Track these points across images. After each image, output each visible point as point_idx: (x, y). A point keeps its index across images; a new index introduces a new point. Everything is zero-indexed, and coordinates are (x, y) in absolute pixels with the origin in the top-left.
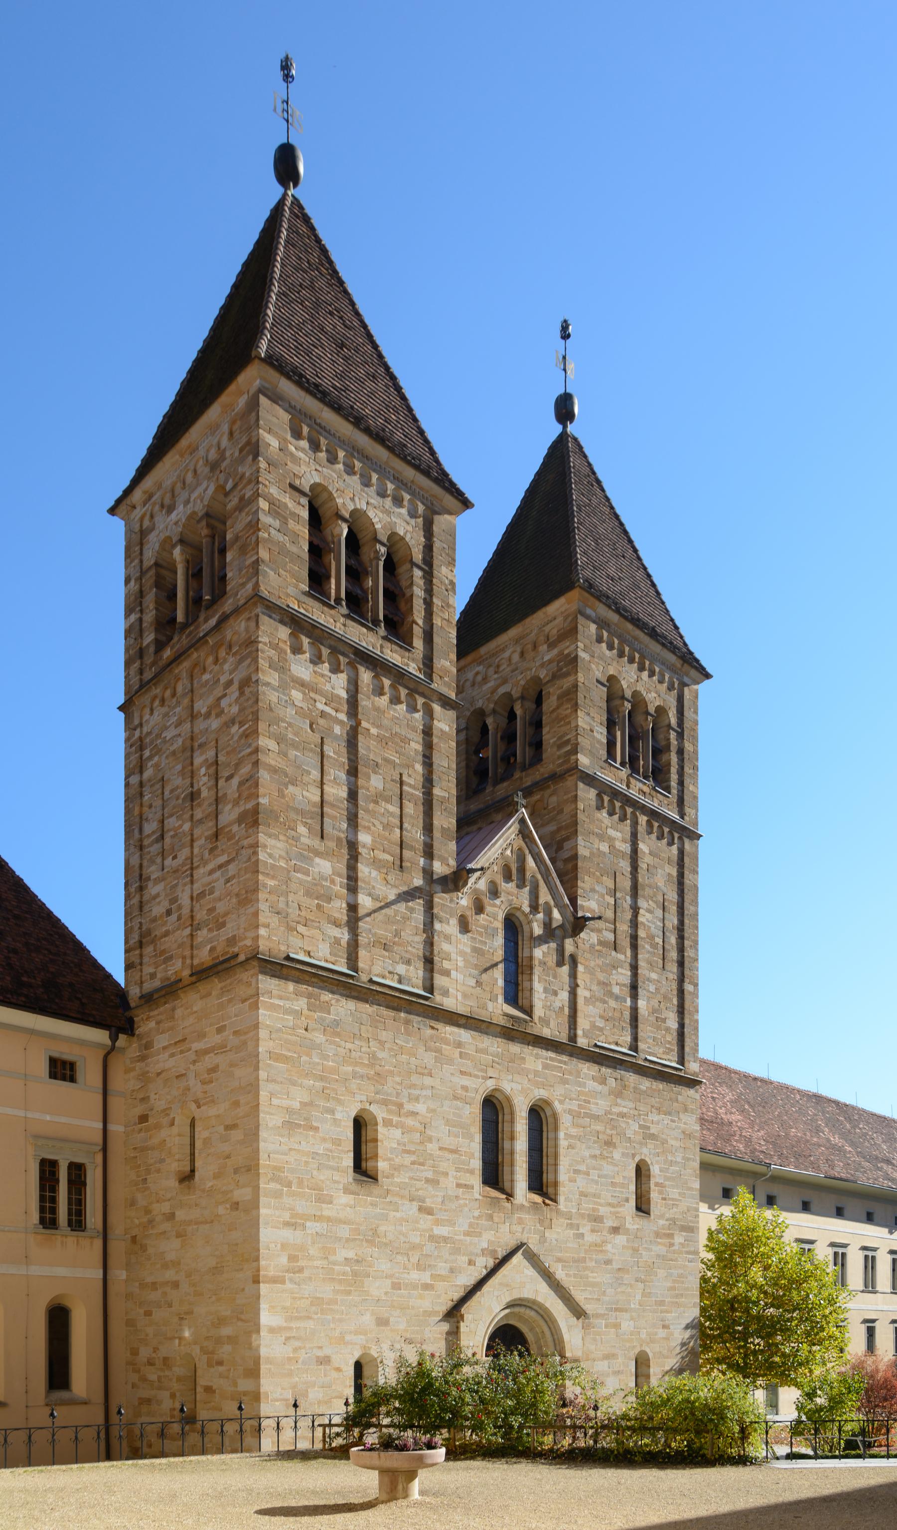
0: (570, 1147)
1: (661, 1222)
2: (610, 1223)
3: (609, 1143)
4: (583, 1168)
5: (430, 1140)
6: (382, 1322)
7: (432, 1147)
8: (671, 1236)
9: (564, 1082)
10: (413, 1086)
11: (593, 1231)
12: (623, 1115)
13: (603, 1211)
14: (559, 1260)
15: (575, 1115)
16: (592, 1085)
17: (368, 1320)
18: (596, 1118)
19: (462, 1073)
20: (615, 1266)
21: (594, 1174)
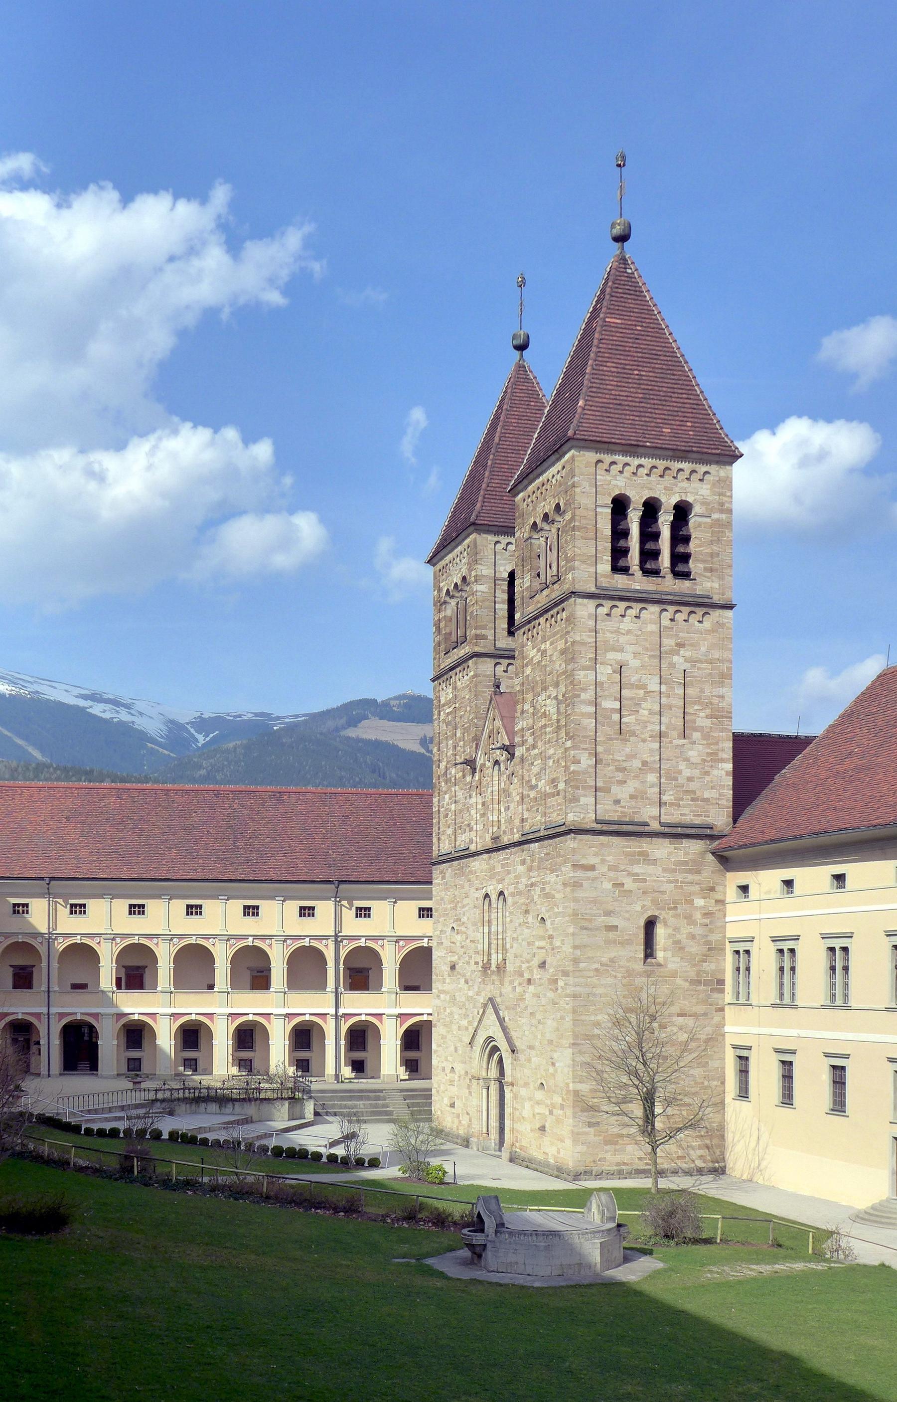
0: (511, 921)
1: (551, 970)
2: (527, 976)
3: (527, 912)
4: (515, 936)
5: (467, 938)
6: (456, 1050)
7: (468, 941)
8: (556, 981)
9: (509, 873)
10: (464, 906)
11: (520, 984)
12: (532, 885)
13: (524, 966)
14: (507, 1008)
15: (513, 895)
16: (521, 868)
17: (452, 1048)
18: (520, 893)
19: (477, 889)
20: (530, 1010)
21: (520, 938)
